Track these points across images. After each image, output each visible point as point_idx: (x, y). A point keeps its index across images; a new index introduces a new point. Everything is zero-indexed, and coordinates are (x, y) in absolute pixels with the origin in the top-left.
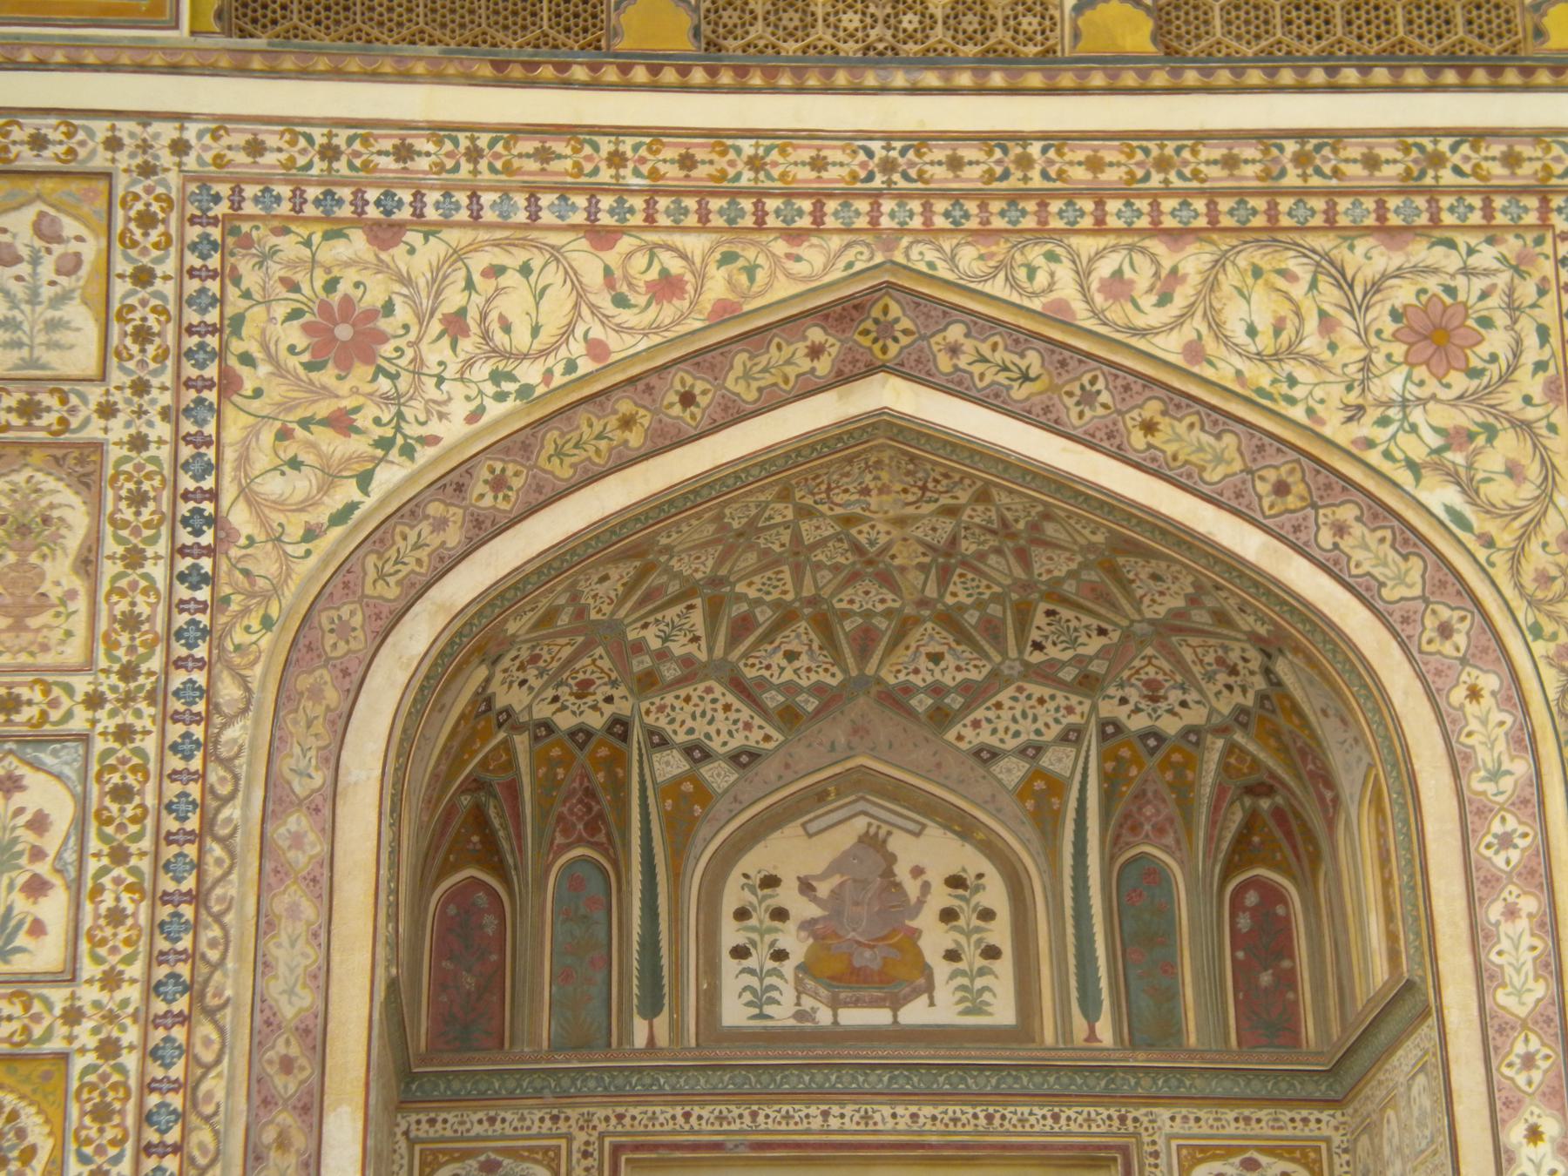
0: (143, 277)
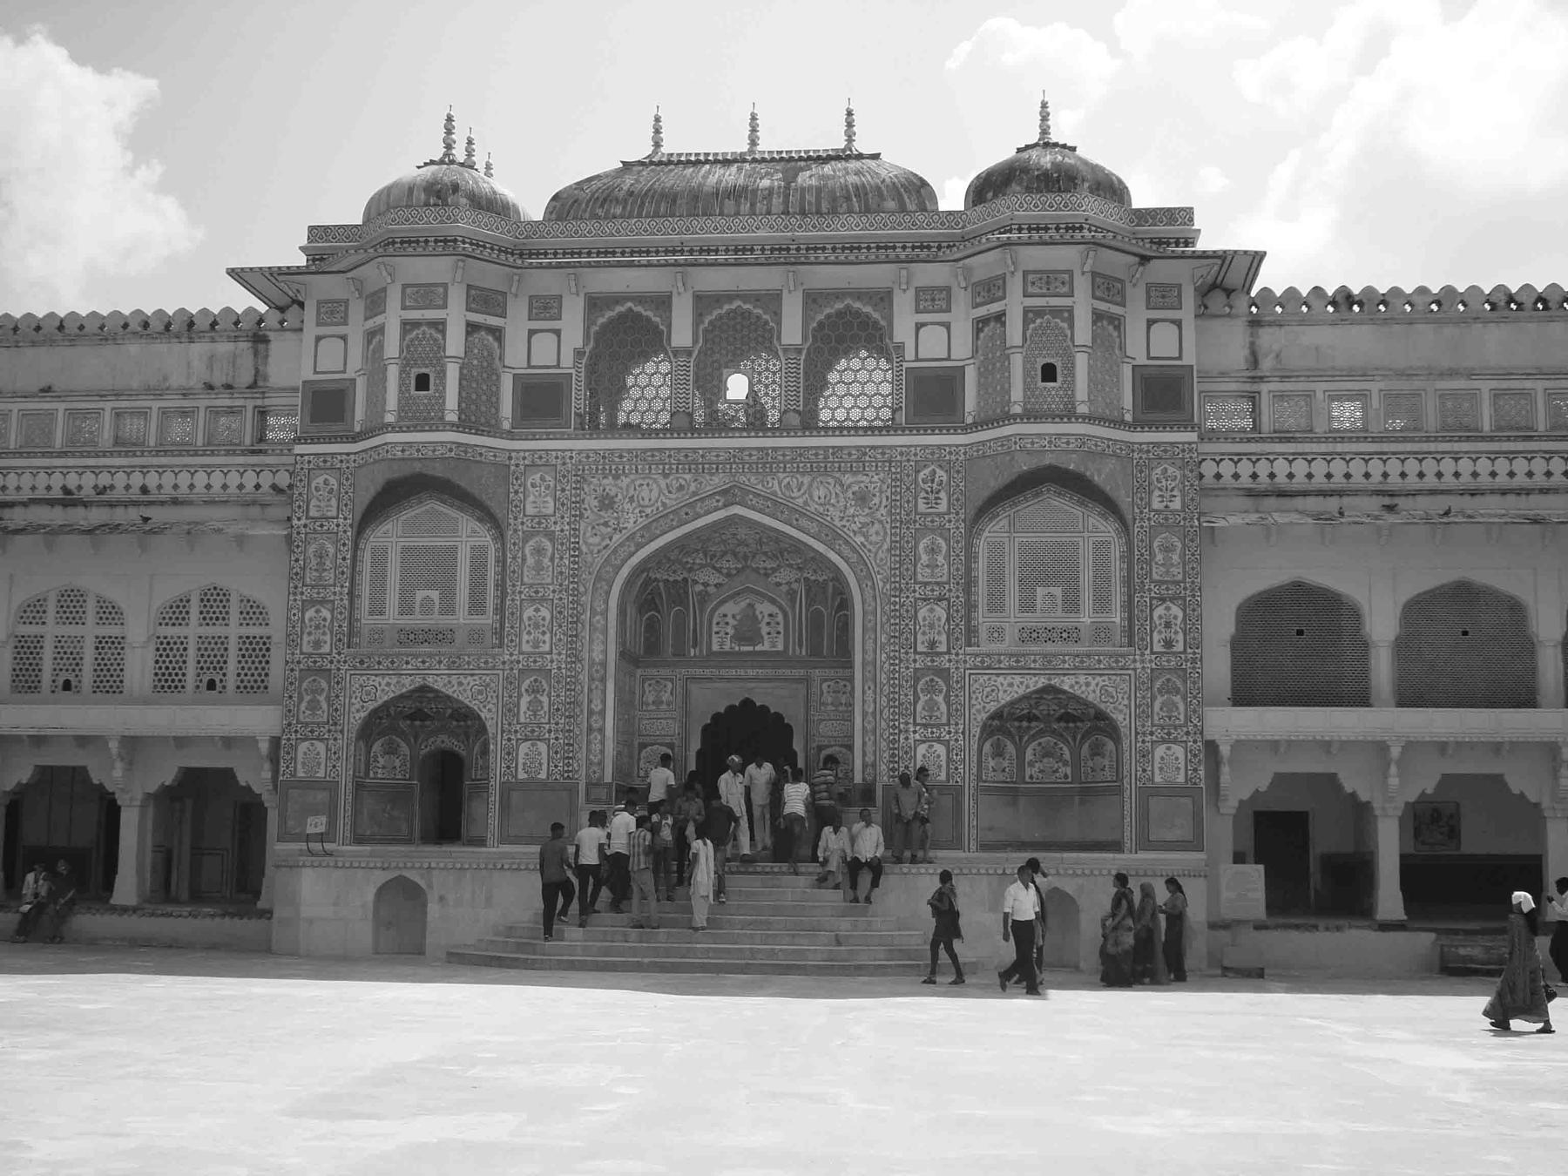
0: (563, 490)
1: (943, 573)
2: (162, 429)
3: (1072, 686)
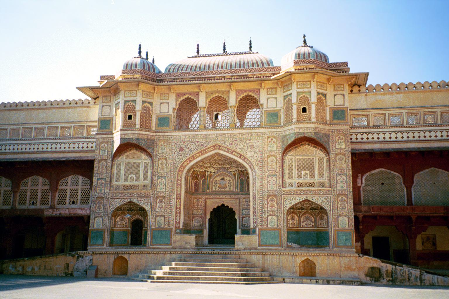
1: (275, 167)
3: (313, 199)
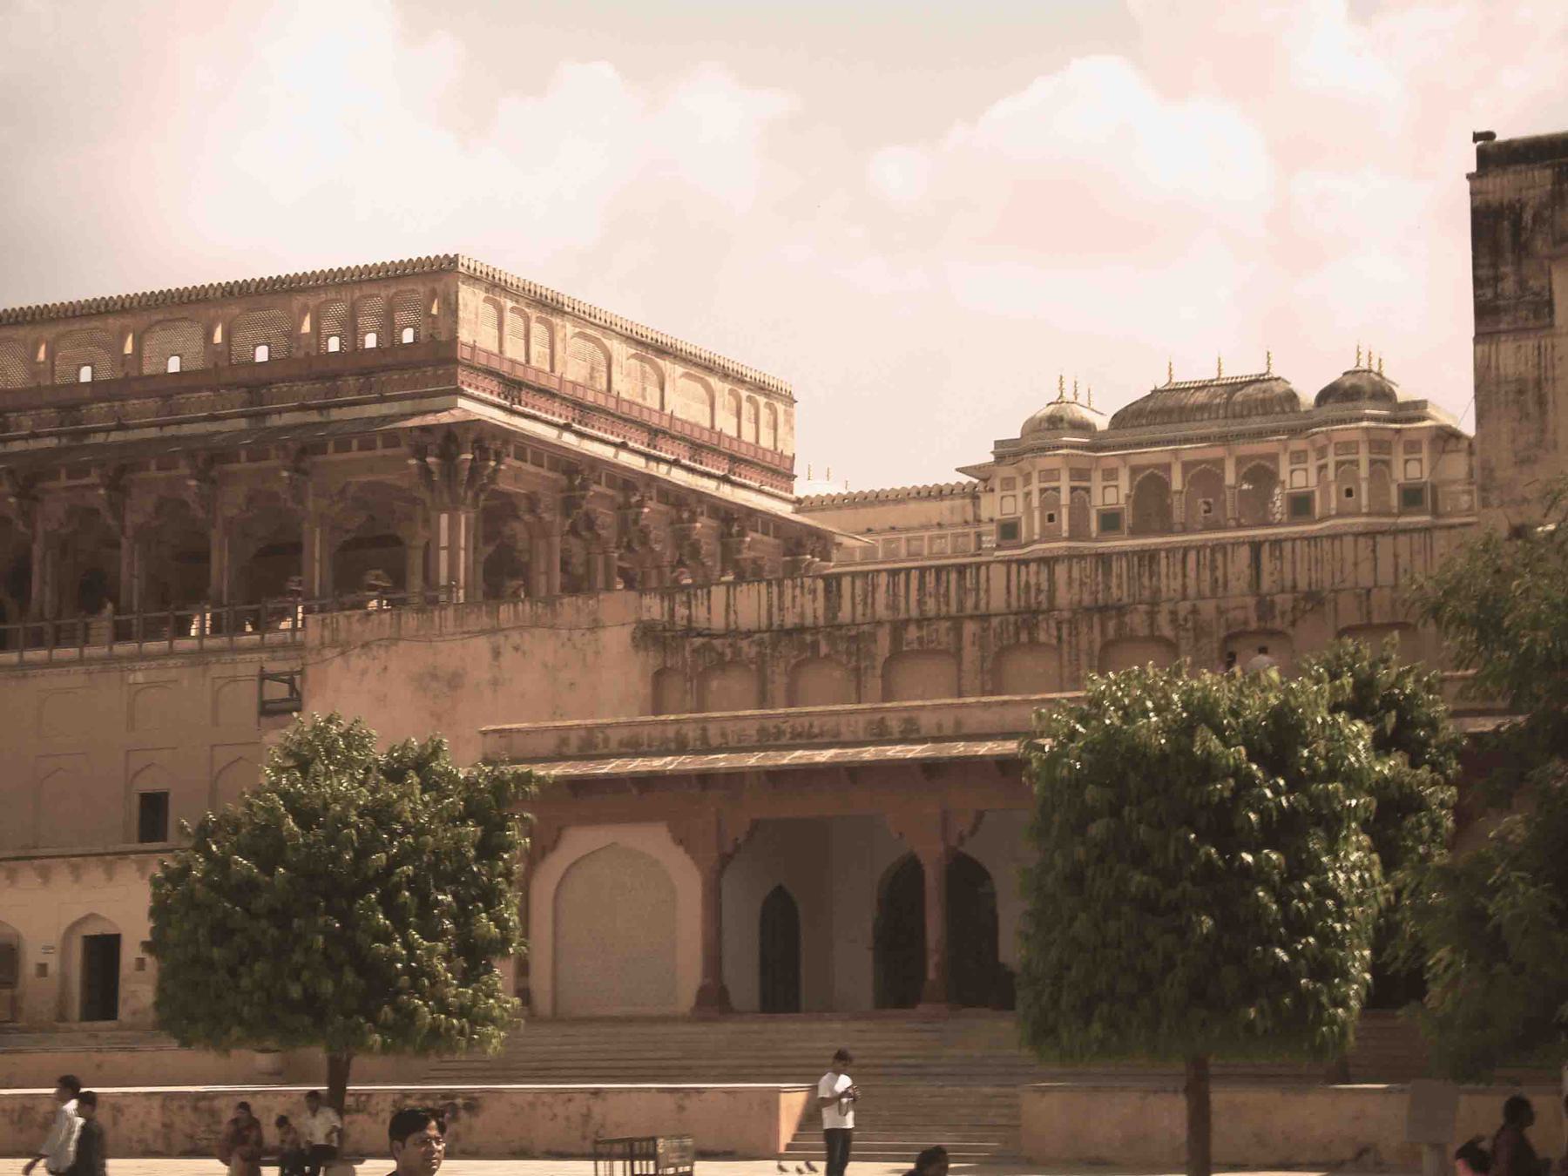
2: (931, 547)
